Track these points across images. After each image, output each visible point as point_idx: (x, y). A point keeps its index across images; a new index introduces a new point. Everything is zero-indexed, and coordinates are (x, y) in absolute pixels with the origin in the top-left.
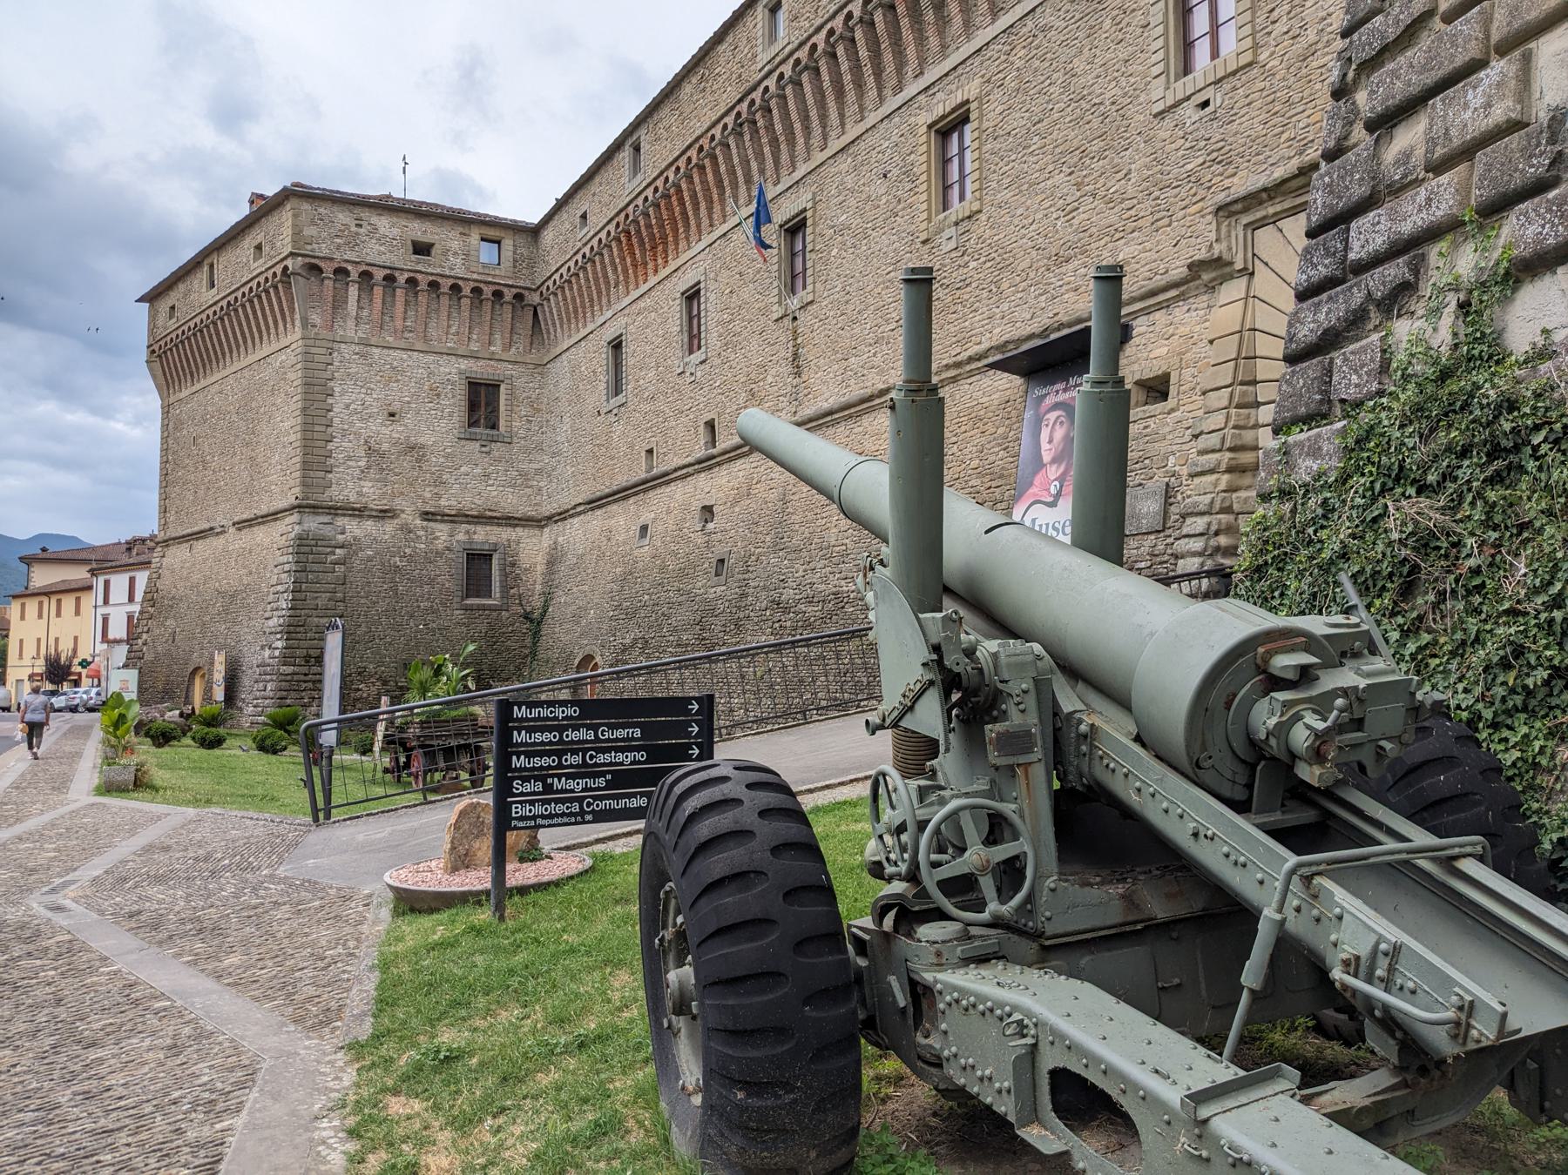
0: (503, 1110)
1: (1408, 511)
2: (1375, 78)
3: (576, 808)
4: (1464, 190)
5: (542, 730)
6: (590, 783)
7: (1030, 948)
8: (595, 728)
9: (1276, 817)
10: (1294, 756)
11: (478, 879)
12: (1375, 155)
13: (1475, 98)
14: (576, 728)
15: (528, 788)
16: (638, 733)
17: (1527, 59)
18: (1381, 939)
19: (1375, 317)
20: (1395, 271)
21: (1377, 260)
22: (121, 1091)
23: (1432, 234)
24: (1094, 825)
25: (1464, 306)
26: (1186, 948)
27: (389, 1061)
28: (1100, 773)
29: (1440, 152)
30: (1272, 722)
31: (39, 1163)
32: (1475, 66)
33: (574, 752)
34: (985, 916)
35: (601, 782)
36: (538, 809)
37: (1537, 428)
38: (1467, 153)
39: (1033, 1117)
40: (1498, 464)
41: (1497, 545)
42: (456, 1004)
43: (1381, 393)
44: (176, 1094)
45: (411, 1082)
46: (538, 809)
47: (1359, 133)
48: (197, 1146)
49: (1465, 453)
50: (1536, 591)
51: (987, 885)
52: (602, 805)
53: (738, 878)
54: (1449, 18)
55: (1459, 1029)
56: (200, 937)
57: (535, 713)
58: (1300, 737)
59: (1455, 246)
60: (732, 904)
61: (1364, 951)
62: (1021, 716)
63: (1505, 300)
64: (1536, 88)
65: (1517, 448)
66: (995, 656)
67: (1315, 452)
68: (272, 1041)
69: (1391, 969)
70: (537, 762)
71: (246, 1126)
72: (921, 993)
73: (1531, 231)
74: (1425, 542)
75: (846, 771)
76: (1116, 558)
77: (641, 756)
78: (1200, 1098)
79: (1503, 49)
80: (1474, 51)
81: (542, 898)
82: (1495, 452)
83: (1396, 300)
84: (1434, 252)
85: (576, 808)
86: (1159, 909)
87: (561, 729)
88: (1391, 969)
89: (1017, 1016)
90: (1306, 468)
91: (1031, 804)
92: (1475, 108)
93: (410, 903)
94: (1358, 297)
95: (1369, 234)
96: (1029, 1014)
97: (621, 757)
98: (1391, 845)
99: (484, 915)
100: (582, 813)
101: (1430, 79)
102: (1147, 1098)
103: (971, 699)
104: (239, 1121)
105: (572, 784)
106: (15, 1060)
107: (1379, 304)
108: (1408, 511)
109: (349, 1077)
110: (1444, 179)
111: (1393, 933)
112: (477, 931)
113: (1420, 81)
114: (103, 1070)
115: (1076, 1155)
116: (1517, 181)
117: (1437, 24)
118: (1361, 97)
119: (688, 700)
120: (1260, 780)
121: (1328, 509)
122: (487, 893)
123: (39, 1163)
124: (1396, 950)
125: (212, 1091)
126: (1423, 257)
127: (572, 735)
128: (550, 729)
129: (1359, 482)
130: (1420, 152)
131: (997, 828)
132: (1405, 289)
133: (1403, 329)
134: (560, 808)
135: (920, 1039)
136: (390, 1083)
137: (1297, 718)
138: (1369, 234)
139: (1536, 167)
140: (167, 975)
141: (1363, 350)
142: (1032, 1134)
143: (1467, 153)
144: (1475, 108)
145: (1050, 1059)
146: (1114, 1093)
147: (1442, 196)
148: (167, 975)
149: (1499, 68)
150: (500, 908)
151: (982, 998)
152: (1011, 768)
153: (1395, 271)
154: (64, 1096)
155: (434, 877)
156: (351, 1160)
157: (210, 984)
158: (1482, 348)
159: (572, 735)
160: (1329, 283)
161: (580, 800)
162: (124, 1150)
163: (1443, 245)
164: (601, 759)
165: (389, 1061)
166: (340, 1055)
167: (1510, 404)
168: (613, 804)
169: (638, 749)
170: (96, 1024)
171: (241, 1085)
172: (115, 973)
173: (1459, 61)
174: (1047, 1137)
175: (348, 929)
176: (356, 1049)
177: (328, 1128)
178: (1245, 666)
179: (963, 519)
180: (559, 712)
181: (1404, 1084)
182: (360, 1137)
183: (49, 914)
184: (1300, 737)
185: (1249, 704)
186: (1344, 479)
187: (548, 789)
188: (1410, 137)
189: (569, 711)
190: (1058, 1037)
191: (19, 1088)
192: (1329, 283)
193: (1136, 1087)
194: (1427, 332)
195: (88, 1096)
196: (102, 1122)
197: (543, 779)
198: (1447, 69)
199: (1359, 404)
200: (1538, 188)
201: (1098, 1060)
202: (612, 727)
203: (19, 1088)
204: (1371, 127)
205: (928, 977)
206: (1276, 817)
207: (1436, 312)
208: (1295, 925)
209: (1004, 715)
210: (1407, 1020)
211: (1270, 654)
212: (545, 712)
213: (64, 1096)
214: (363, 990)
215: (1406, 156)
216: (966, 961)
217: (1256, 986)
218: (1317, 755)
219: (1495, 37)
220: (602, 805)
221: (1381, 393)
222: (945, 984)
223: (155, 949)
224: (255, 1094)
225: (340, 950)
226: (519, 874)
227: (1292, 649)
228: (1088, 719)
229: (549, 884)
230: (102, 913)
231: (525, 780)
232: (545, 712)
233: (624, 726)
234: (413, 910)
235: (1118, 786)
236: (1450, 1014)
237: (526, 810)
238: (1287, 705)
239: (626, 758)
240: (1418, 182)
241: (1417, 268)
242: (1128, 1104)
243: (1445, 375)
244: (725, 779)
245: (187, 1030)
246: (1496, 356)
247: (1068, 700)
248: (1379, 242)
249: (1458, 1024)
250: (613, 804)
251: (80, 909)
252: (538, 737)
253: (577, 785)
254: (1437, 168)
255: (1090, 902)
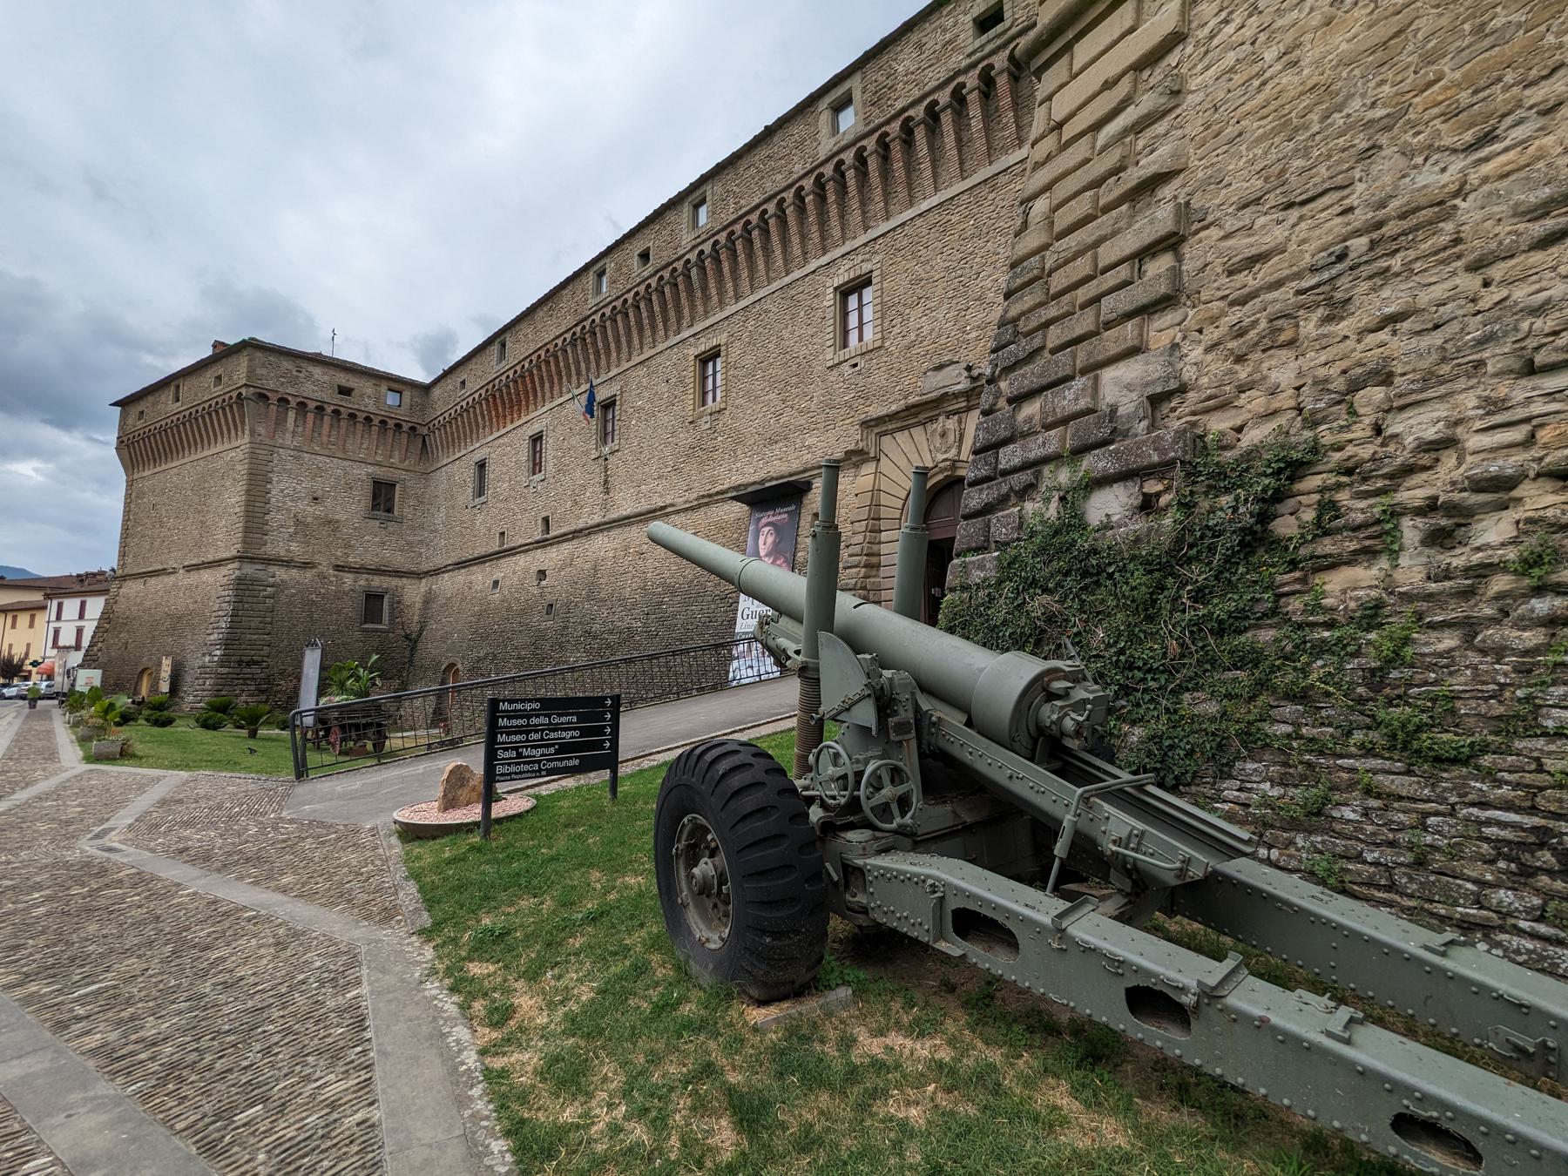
0: (557, 964)
1: (1039, 604)
2: (1012, 376)
3: (536, 767)
4: (1063, 440)
5: (517, 717)
6: (545, 751)
7: (908, 842)
8: (549, 716)
9: (1052, 766)
10: (1063, 734)
11: (474, 813)
12: (1013, 416)
13: (1069, 394)
14: (537, 716)
15: (507, 755)
16: (575, 719)
17: (1096, 378)
18: (1134, 828)
19: (1013, 500)
20: (1026, 477)
21: (1015, 470)
22: (252, 980)
23: (1045, 460)
24: (945, 774)
25: (1062, 499)
26: (1009, 836)
27: (454, 940)
28: (942, 743)
29: (1050, 419)
30: (1055, 717)
31: (213, 1039)
32: (1069, 378)
33: (536, 731)
34: (894, 825)
35: (552, 750)
36: (513, 769)
37: (1110, 564)
38: (1064, 421)
39: (941, 936)
40: (1088, 580)
41: (1086, 621)
42: (486, 898)
43: (1018, 539)
44: (301, 977)
45: (479, 950)
46: (513, 769)
47: (1002, 403)
48: (340, 1011)
49: (1067, 574)
50: (1109, 646)
51: (895, 807)
52: (552, 765)
53: (761, 811)
54: (1054, 352)
55: (1182, 872)
56: (256, 864)
57: (513, 707)
58: (1069, 724)
59: (1057, 467)
60: (759, 826)
61: (1124, 835)
62: (905, 714)
63: (1086, 498)
64: (1101, 393)
65: (1098, 574)
66: (891, 679)
67: (982, 567)
68: (357, 933)
69: (1139, 843)
70: (514, 738)
71: (372, 993)
72: (853, 874)
73: (1101, 465)
74: (1050, 618)
75: (675, 740)
76: (932, 621)
77: (576, 733)
78: (1061, 916)
79: (1084, 372)
80: (1068, 371)
81: (513, 826)
82: (1085, 574)
83: (1026, 492)
84: (1046, 470)
85: (536, 767)
86: (968, 818)
87: (529, 717)
88: (1139, 843)
89: (930, 882)
90: (977, 576)
91: (909, 761)
92: (1070, 399)
93: (412, 833)
94: (1005, 489)
95: (1010, 456)
96: (939, 880)
97: (564, 734)
98: (1112, 781)
99: (475, 839)
100: (540, 770)
101: (1044, 381)
102: (1025, 920)
103: (884, 702)
104: (364, 989)
105: (534, 752)
106: (145, 966)
107: (1016, 493)
108: (1039, 604)
109: (429, 952)
110: (1052, 433)
111: (1141, 826)
112: (473, 848)
113: (1037, 382)
114: (229, 964)
115: (970, 955)
116: (1092, 439)
117: (1046, 354)
118: (1003, 385)
119: (605, 698)
120: (1048, 748)
121: (991, 599)
122: (476, 824)
123: (213, 1039)
124: (1143, 833)
125: (330, 972)
126: (1040, 471)
127: (534, 721)
128: (521, 717)
129: (1008, 585)
130: (1037, 417)
131: (896, 774)
132: (1031, 487)
133: (1029, 506)
134: (526, 768)
135: (848, 897)
136: (464, 954)
137: (1066, 714)
138: (1010, 456)
139: (1105, 432)
140: (239, 893)
141: (1008, 516)
142: (942, 946)
143: (1064, 421)
144: (1070, 399)
145: (953, 904)
146: (1000, 919)
147: (1052, 442)
148: (239, 893)
149: (1079, 383)
150: (486, 834)
151: (904, 873)
152: (900, 742)
153: (1026, 477)
154: (206, 987)
155: (430, 814)
156: (461, 1006)
157: (279, 897)
158: (1074, 521)
159: (534, 721)
160: (988, 479)
161: (539, 762)
162: (282, 1021)
163: (1051, 467)
164: (552, 735)
165: (454, 940)
166: (414, 938)
167: (1094, 551)
168: (559, 764)
169: (574, 729)
170: (202, 933)
171: (350, 965)
172: (195, 894)
173: (1060, 375)
174: (952, 947)
175: (368, 854)
176: (426, 934)
177: (432, 988)
178: (1039, 689)
179: (845, 602)
180: (528, 706)
181: (1130, 902)
182: (460, 992)
183: (107, 855)
184: (1069, 724)
185: (1040, 706)
186: (1000, 582)
187: (519, 755)
188: (1031, 409)
189: (534, 706)
190: (960, 891)
191: (161, 986)
192: (988, 479)
193: (1017, 914)
194: (1042, 510)
195: (227, 986)
196: (250, 1003)
197: (516, 749)
198: (1053, 378)
199: (1007, 544)
200: (1105, 443)
201: (989, 902)
202: (559, 715)
203: (161, 986)
204: (1010, 401)
205: (860, 862)
206: (1052, 766)
207: (1047, 500)
208: (1084, 825)
209: (896, 713)
210: (1155, 871)
211: (1050, 681)
212: (519, 706)
213: (206, 987)
214: (409, 894)
215: (1030, 419)
216: (879, 852)
217: (1064, 856)
218: (1078, 734)
219: (1079, 365)
220: (552, 765)
221: (1018, 539)
222: (874, 866)
223: (215, 875)
224: (365, 971)
225: (371, 867)
226: (498, 810)
227: (1058, 679)
228: (938, 714)
229: (514, 816)
230: (153, 851)
231: (506, 749)
232: (519, 706)
233: (567, 715)
234: (419, 838)
235: (955, 751)
236: (1178, 865)
237: (505, 770)
238: (1062, 708)
239: (567, 735)
240: (1036, 433)
241: (1038, 475)
242: (1009, 925)
243: (1056, 533)
244: (736, 752)
245: (281, 931)
246: (1083, 526)
247: (925, 704)
248: (1016, 461)
249: (1181, 870)
250: (559, 764)
251: (132, 849)
252: (515, 722)
253: (537, 753)
254: (1048, 427)
255: (941, 815)
